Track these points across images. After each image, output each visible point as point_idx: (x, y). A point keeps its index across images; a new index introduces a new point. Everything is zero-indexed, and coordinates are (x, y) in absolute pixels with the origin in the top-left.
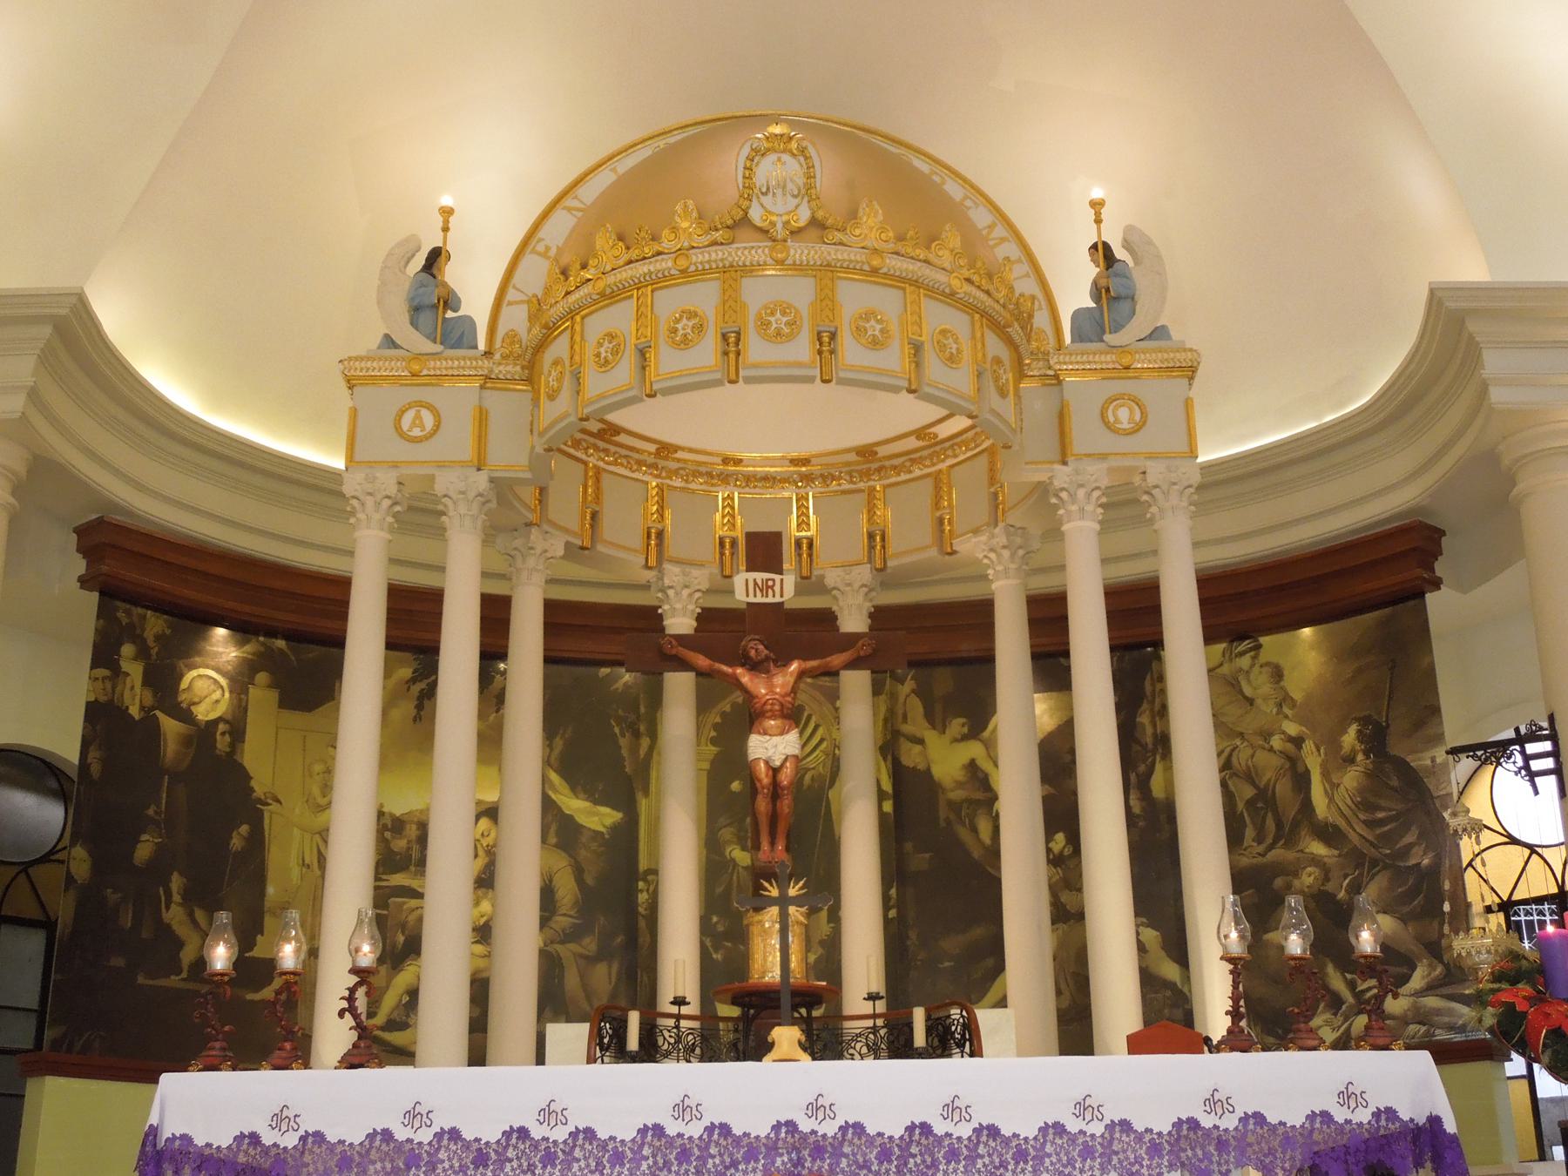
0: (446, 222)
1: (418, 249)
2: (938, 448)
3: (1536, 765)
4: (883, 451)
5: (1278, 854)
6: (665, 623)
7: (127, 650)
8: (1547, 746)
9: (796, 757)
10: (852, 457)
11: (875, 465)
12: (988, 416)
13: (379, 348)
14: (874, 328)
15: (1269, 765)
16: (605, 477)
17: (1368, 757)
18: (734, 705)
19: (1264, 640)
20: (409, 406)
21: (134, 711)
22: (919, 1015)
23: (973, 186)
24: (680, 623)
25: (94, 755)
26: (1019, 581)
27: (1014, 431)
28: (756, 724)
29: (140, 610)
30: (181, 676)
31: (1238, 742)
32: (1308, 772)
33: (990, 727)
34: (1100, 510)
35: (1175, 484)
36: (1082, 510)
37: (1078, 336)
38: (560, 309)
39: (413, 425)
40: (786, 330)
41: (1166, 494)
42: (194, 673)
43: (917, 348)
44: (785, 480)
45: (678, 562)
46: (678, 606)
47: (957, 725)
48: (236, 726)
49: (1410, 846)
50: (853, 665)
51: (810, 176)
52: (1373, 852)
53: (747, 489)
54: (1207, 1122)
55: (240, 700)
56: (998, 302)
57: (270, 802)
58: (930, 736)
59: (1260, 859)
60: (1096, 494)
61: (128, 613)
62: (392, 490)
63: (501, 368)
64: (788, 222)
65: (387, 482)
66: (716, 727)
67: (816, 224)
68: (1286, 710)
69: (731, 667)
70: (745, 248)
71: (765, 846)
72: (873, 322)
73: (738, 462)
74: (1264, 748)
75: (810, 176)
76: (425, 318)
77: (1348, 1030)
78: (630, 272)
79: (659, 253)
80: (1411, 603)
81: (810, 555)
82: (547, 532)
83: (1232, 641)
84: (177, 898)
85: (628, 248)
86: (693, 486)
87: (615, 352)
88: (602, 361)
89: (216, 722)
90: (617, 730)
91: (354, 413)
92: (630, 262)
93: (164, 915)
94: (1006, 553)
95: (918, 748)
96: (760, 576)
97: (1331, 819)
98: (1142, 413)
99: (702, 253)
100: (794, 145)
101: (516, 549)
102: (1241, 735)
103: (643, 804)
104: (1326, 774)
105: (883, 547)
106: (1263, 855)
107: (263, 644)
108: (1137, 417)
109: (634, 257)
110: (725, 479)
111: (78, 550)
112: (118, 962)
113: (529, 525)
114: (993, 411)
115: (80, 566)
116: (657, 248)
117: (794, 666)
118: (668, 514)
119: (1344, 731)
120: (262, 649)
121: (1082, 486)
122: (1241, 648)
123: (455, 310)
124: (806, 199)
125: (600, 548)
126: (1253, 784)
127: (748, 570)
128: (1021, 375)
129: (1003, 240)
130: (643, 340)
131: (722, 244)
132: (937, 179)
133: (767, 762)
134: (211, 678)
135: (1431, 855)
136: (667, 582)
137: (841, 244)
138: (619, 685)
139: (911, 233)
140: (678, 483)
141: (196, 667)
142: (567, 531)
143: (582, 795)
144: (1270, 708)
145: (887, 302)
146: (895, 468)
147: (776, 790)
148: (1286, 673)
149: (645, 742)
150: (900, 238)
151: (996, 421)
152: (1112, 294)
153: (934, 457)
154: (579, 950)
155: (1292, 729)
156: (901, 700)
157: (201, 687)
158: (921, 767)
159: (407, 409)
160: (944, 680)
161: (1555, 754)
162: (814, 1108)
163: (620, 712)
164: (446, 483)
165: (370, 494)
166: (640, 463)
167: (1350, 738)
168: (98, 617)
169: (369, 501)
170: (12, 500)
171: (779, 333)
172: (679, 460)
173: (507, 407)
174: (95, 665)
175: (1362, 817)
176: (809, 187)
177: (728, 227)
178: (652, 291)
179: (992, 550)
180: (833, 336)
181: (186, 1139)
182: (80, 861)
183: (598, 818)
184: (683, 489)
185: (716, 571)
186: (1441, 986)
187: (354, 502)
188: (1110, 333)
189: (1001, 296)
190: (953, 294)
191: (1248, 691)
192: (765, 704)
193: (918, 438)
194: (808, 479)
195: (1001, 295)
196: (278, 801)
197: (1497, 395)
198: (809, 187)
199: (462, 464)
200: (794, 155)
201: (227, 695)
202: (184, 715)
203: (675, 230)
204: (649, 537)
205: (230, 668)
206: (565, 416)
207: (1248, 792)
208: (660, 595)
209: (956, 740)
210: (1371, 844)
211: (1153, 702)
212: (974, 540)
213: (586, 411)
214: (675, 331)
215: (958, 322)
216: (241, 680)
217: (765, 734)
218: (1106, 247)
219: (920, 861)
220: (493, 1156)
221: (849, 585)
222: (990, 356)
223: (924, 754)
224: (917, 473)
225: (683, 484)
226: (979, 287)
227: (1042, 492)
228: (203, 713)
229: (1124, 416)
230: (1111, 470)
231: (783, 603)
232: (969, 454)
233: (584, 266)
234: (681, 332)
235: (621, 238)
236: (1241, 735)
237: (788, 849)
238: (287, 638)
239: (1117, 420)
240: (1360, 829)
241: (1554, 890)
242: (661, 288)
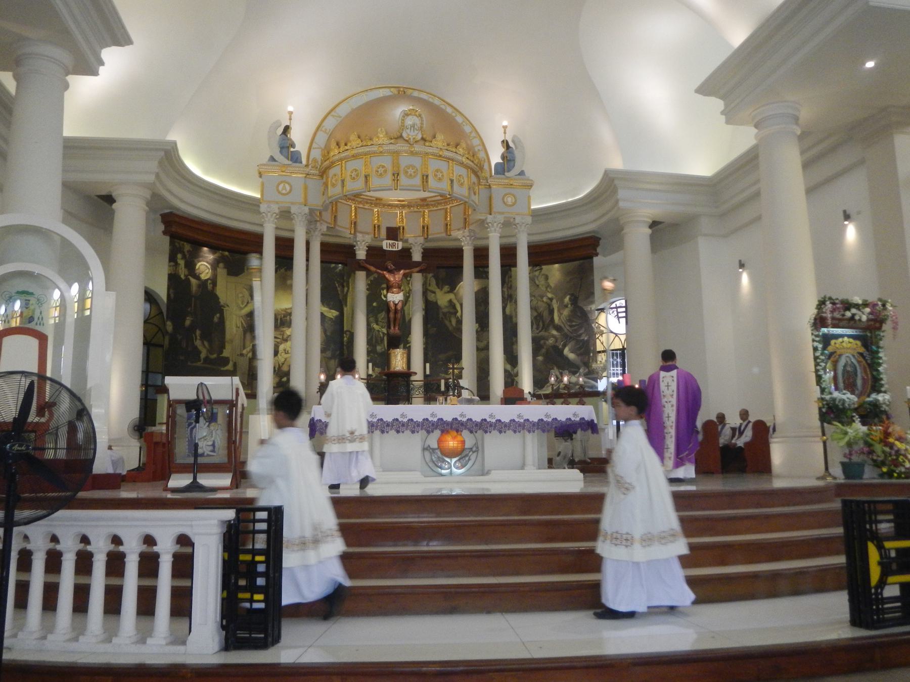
0: (290, 117)
1: (280, 125)
2: (447, 200)
3: (620, 315)
4: (428, 200)
5: (543, 333)
6: (357, 252)
7: (179, 256)
8: (624, 309)
9: (402, 300)
10: (419, 200)
11: (425, 203)
12: (472, 203)
13: (269, 160)
14: (440, 175)
15: (542, 307)
16: (339, 204)
17: (572, 306)
18: (374, 277)
19: (544, 267)
20: (282, 182)
21: (183, 277)
22: (443, 382)
23: (465, 117)
24: (361, 254)
25: (171, 291)
26: (470, 247)
27: (477, 206)
28: (390, 290)
29: (182, 242)
30: (196, 265)
32: (553, 309)
33: (457, 288)
34: (500, 230)
35: (523, 223)
36: (495, 230)
37: (497, 172)
38: (336, 158)
39: (283, 189)
40: (413, 174)
41: (521, 226)
42: (200, 264)
43: (452, 181)
44: (397, 206)
45: (361, 232)
46: (361, 247)
47: (446, 288)
48: (214, 281)
50: (418, 272)
51: (422, 124)
52: (572, 335)
53: (383, 209)
54: (545, 420)
55: (214, 274)
56: (475, 164)
57: (225, 306)
58: (438, 291)
59: (537, 335)
60: (500, 225)
61: (179, 243)
62: (277, 211)
63: (311, 171)
64: (414, 138)
65: (275, 208)
66: (368, 285)
67: (423, 139)
68: (549, 289)
69: (382, 270)
70: (403, 146)
71: (392, 328)
72: (439, 173)
73: (380, 199)
74: (540, 301)
75: (422, 124)
76: (285, 150)
77: (559, 387)
78: (363, 150)
79: (372, 145)
80: (589, 260)
81: (403, 232)
82: (321, 223)
83: (533, 267)
84: (198, 337)
85: (362, 141)
86: (365, 207)
87: (357, 175)
88: (352, 178)
89: (207, 280)
90: (337, 285)
91: (263, 184)
92: (362, 146)
93: (195, 343)
94: (468, 238)
95: (433, 295)
96: (391, 242)
97: (559, 324)
98: (516, 201)
99: (387, 146)
100: (417, 114)
101: (311, 229)
102: (534, 296)
103: (346, 310)
104: (559, 311)
105: (427, 231)
106: (538, 333)
107: (221, 254)
108: (514, 201)
109: (364, 144)
110: (376, 205)
111: (162, 222)
112: (182, 358)
113: (316, 221)
114: (473, 201)
115: (162, 227)
116: (372, 143)
117: (402, 272)
118: (358, 217)
119: (565, 298)
120: (221, 255)
121: (495, 222)
123: (294, 148)
124: (420, 132)
125: (337, 228)
127: (388, 238)
128: (479, 184)
129: (475, 137)
130: (367, 173)
131: (393, 144)
132: (454, 114)
133: (393, 302)
134: (205, 265)
135: (588, 337)
136: (358, 239)
137: (431, 146)
138: (338, 270)
139: (452, 143)
140: (361, 206)
141: (199, 261)
142: (326, 222)
143: (326, 306)
144: (544, 289)
145: (443, 165)
146: (432, 205)
147: (396, 311)
148: (549, 278)
149: (346, 289)
150: (448, 145)
151: (473, 204)
152: (508, 158)
153: (446, 203)
154: (325, 355)
155: (550, 295)
156: (428, 279)
157: (202, 268)
158: (435, 301)
159: (281, 183)
160: (443, 273)
161: (626, 312)
162: (462, 415)
163: (338, 279)
164: (294, 210)
165: (269, 212)
166: (349, 199)
167: (567, 299)
168: (170, 245)
169: (269, 214)
170: (147, 208)
171: (411, 175)
172: (361, 198)
173: (315, 185)
174: (170, 260)
175: (568, 323)
176: (421, 127)
177: (395, 138)
178: (370, 157)
179: (464, 236)
180: (427, 176)
181: (320, 421)
182: (169, 326)
183: (333, 314)
184: (362, 208)
185: (373, 235)
186: (587, 375)
187: (264, 214)
188: (507, 172)
189: (476, 162)
190: (463, 163)
191: (537, 282)
192: (393, 283)
193: (441, 197)
194: (403, 206)
195: (476, 162)
196: (228, 306)
197: (621, 204)
198: (421, 127)
199: (300, 204)
200: (418, 117)
201: (210, 271)
202: (197, 277)
203: (378, 137)
204: (352, 224)
205: (211, 262)
206: (340, 194)
208: (355, 243)
209: (445, 293)
210: (570, 332)
211: (508, 285)
212: (459, 232)
213: (347, 194)
214: (378, 172)
215: (463, 171)
216: (215, 265)
217: (393, 293)
218: (507, 142)
219: (433, 331)
220: (391, 425)
221: (416, 243)
222: (472, 182)
223: (435, 297)
224: (440, 208)
225: (363, 206)
226: (470, 160)
227: (482, 223)
228: (204, 277)
229: (510, 200)
230: (505, 217)
231: (396, 251)
232: (457, 204)
233: (346, 145)
234: (380, 172)
235: (359, 137)
237: (399, 329)
238: (229, 251)
239: (507, 202)
240: (568, 328)
241: (622, 347)
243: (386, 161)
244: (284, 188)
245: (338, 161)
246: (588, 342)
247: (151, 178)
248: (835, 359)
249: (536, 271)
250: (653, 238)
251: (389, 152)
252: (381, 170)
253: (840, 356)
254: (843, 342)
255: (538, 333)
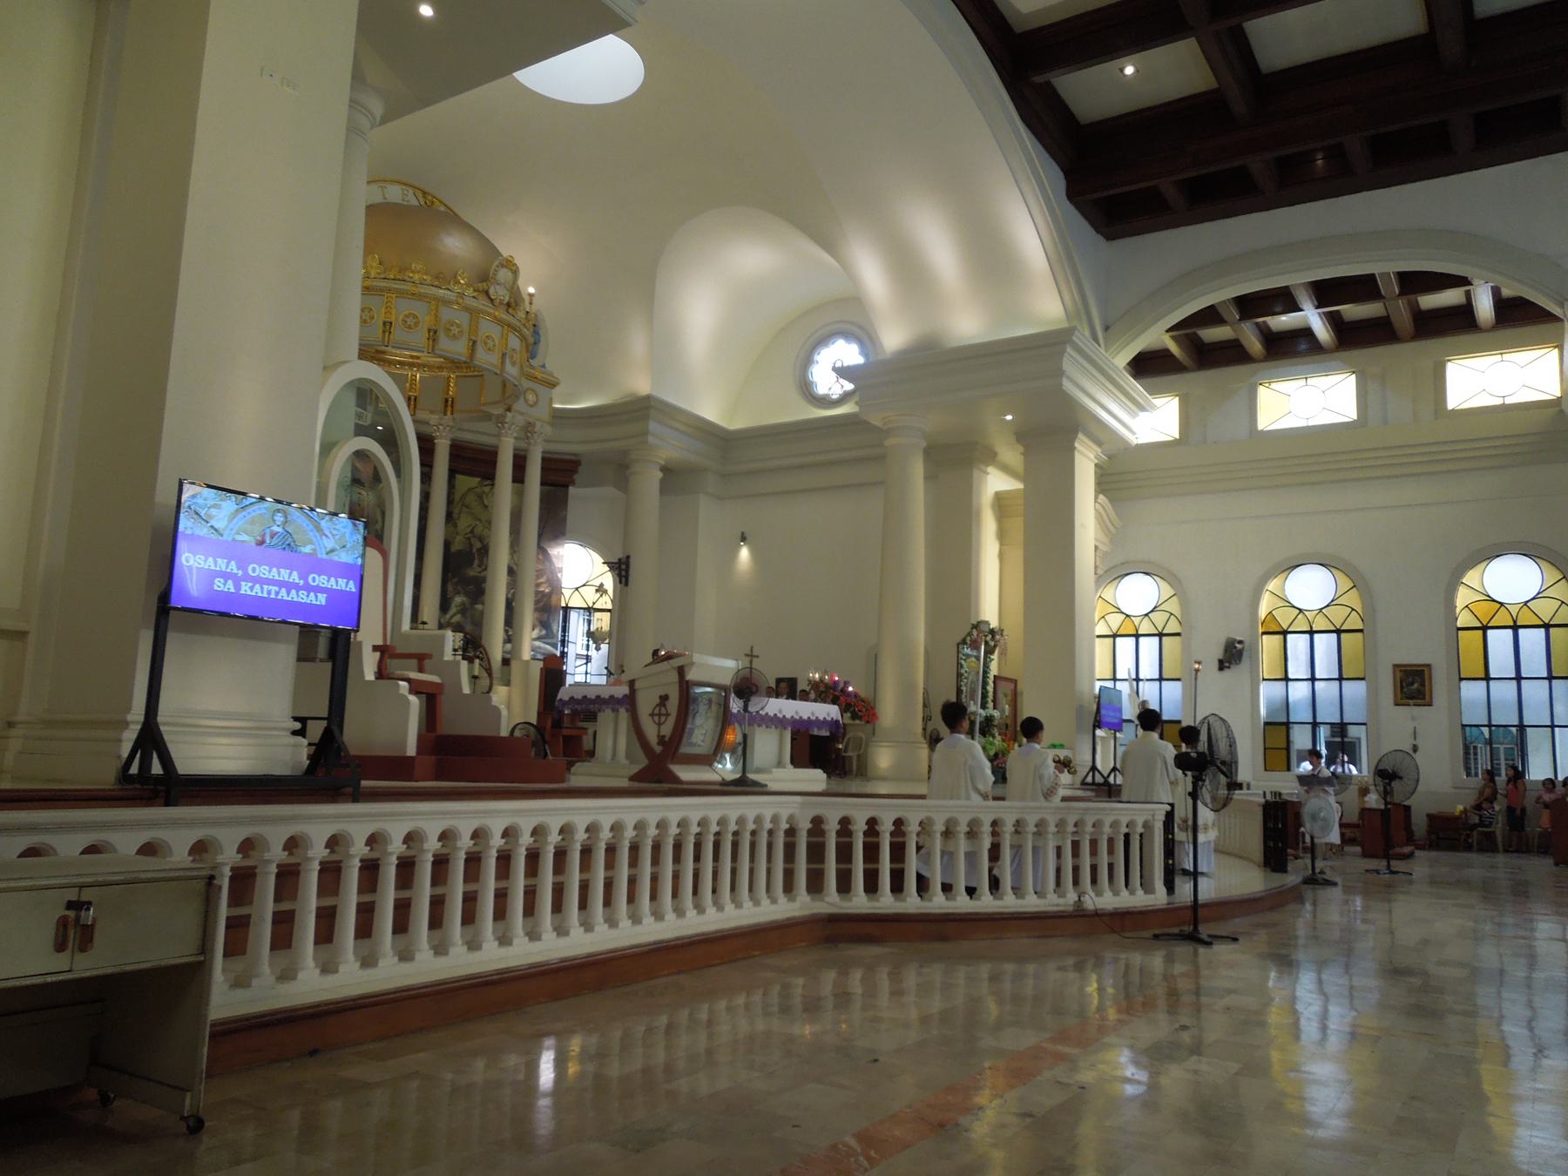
31: (478, 523)
35: (542, 433)
49: (542, 583)
67: (509, 305)
98: (537, 400)
102: (479, 520)
106: (480, 572)
108: (535, 399)
121: (513, 424)
122: (486, 483)
126: (481, 541)
180: (504, 355)
191: (486, 502)
207: (478, 545)
212: (432, 416)
214: (450, 330)
229: (531, 397)
236: (479, 520)
243: (462, 319)
245: (382, 290)
246: (549, 595)
249: (486, 485)
250: (663, 482)
251: (467, 309)
252: (455, 330)
255: (480, 572)
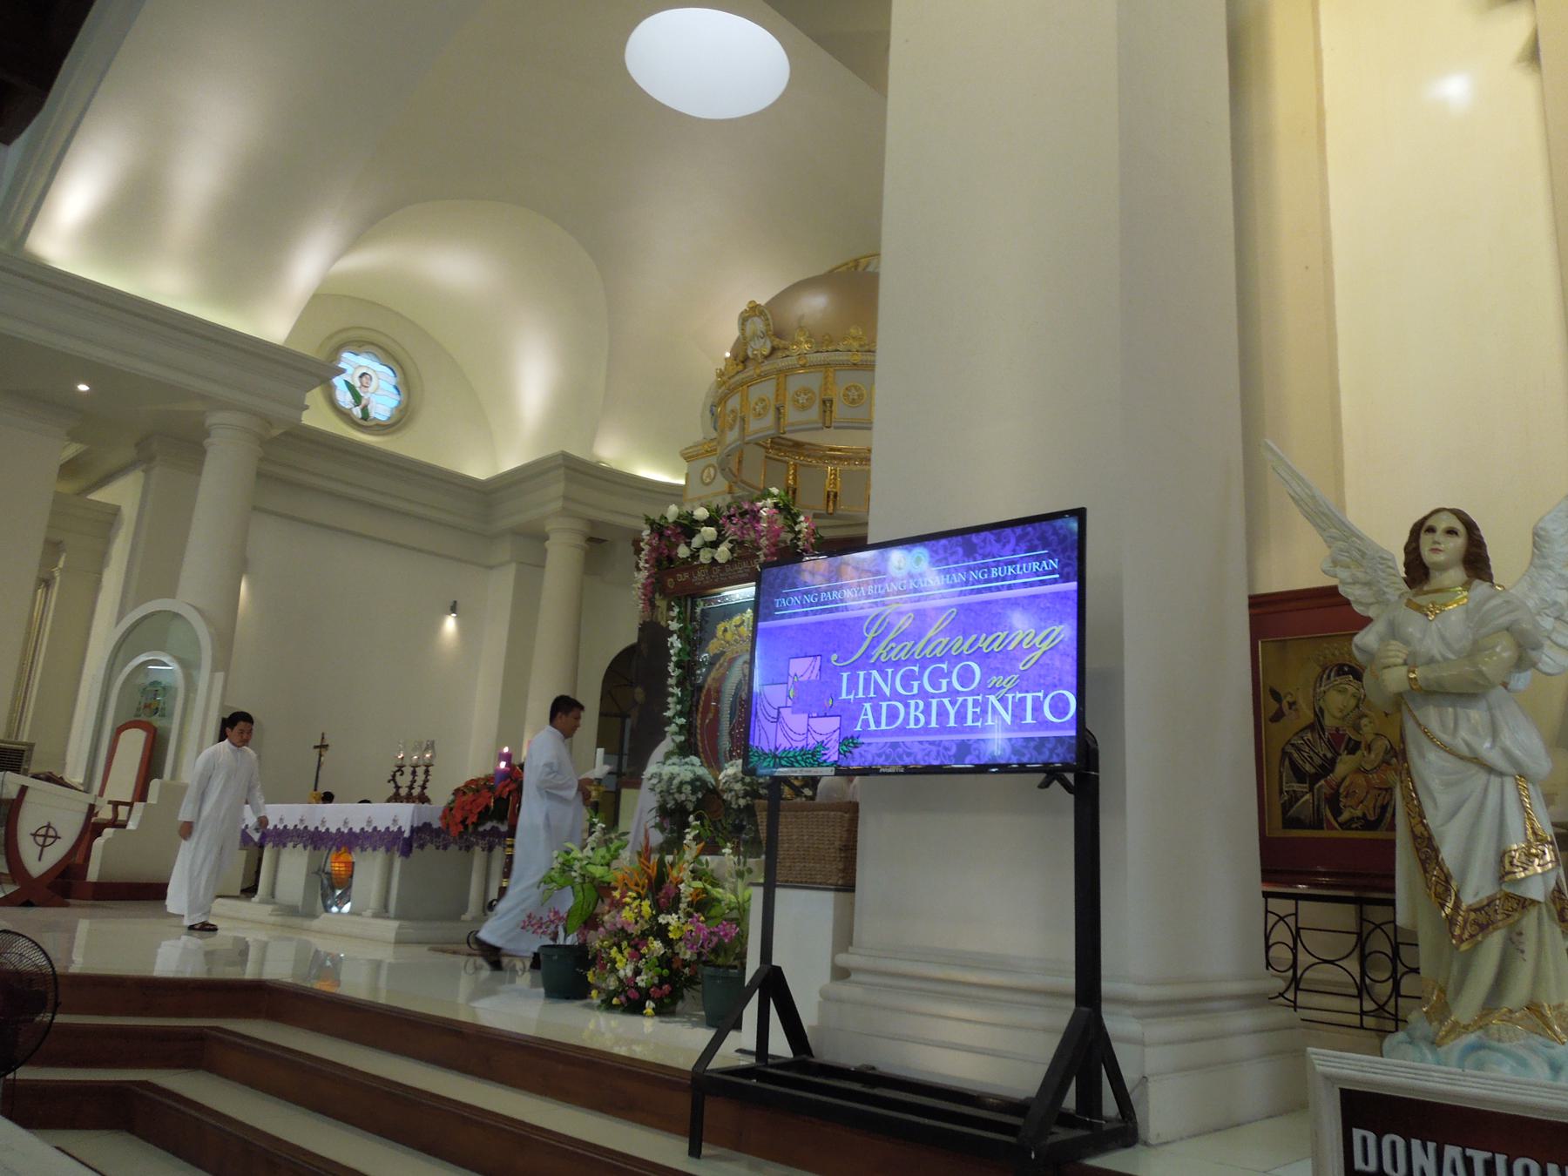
40: (762, 411)
67: (774, 350)
72: (802, 396)
145: (814, 381)
170: (583, 544)
171: (760, 414)
242: (728, 400)
244: (709, 476)
247: (558, 504)
248: (721, 670)
253: (732, 661)
254: (743, 622)
